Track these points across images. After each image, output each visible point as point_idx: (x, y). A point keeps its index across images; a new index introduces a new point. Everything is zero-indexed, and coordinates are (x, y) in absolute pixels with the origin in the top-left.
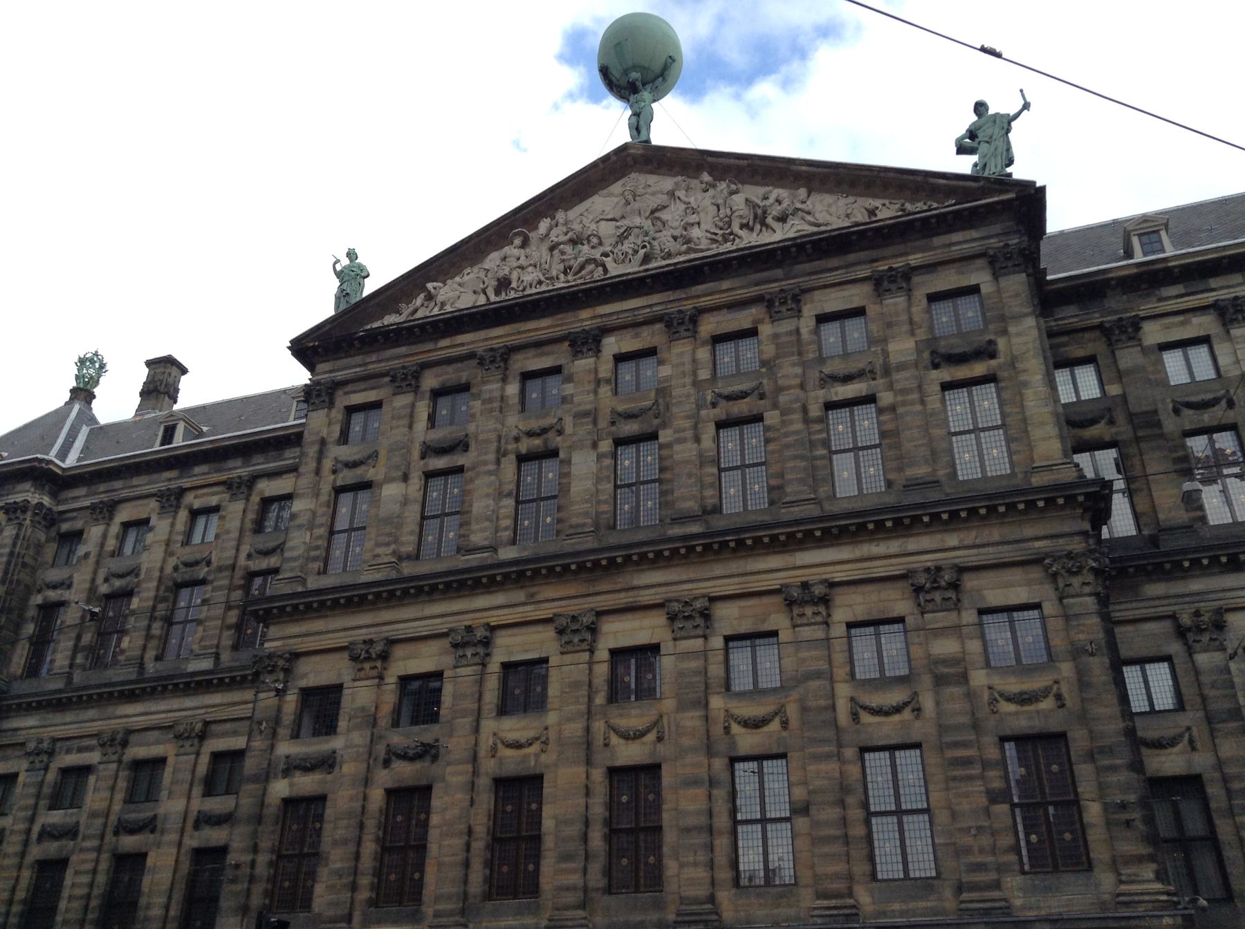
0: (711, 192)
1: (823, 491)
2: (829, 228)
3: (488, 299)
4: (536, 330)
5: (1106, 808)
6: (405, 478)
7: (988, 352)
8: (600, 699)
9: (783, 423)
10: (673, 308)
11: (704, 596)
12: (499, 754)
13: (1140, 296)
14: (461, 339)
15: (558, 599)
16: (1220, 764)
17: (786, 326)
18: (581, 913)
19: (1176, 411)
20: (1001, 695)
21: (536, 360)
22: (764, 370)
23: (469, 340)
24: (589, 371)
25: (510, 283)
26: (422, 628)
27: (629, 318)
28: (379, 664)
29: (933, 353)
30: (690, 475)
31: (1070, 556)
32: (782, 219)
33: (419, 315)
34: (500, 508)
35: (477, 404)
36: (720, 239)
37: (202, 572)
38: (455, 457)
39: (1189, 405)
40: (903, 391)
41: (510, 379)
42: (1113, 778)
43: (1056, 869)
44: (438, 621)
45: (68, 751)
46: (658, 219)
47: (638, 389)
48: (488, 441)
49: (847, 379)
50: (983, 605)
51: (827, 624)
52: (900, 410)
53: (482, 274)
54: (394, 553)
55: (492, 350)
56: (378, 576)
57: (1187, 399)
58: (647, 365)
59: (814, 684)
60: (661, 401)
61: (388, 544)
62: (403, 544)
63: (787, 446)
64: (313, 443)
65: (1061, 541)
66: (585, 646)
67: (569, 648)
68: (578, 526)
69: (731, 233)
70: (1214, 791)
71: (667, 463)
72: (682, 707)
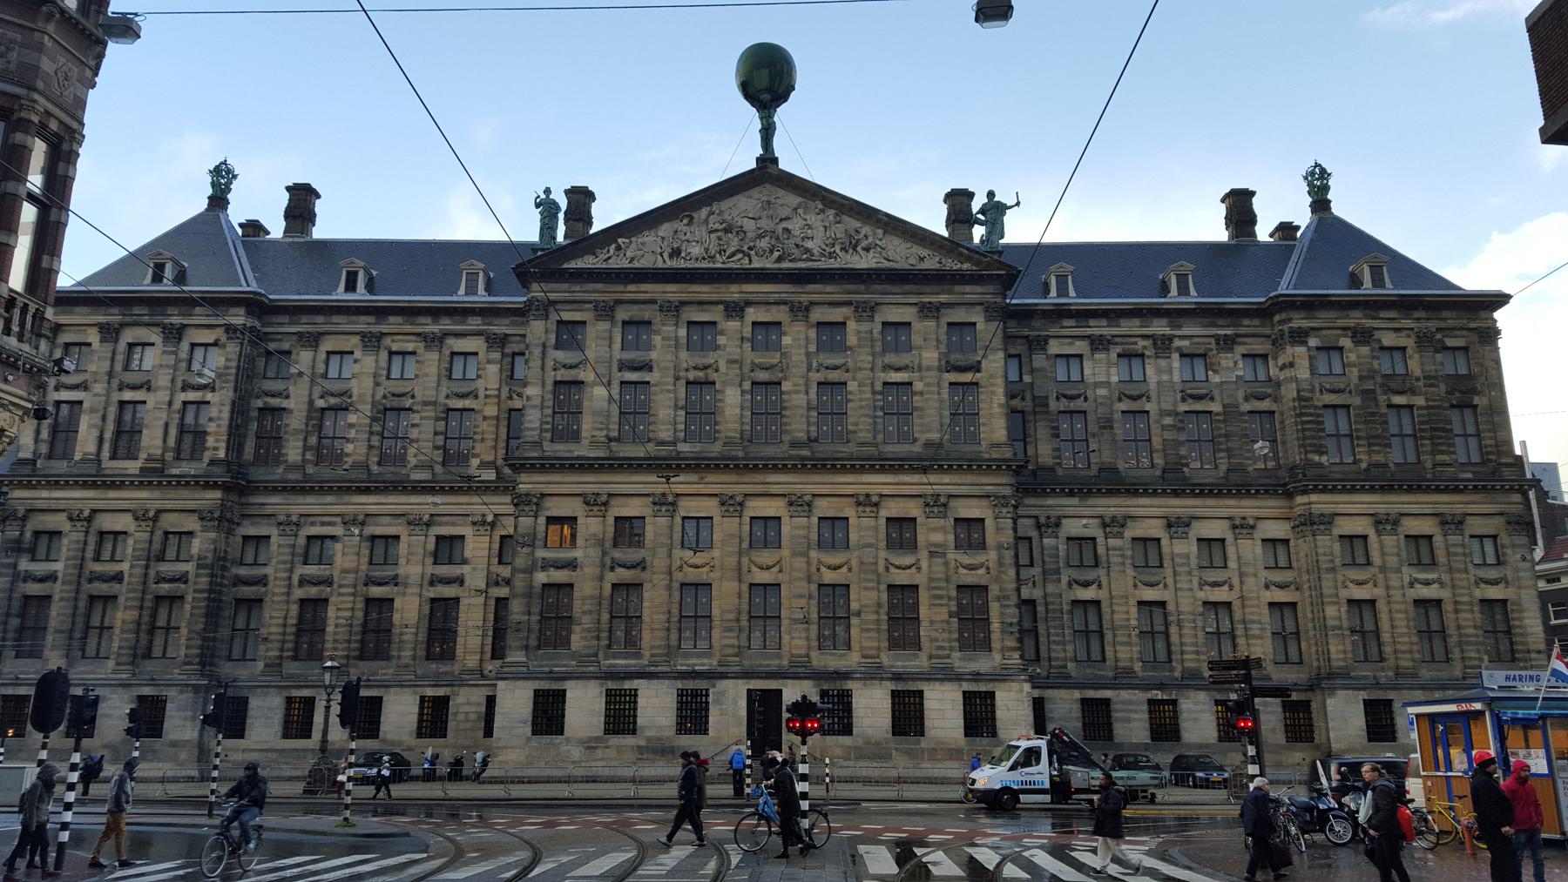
7: (976, 368)
8: (745, 545)
10: (794, 298)
14: (644, 287)
16: (1045, 595)
17: (865, 326)
32: (867, 249)
37: (408, 403)
39: (1065, 396)
40: (929, 385)
45: (313, 524)
48: (667, 368)
49: (898, 369)
70: (1040, 608)
72: (795, 554)
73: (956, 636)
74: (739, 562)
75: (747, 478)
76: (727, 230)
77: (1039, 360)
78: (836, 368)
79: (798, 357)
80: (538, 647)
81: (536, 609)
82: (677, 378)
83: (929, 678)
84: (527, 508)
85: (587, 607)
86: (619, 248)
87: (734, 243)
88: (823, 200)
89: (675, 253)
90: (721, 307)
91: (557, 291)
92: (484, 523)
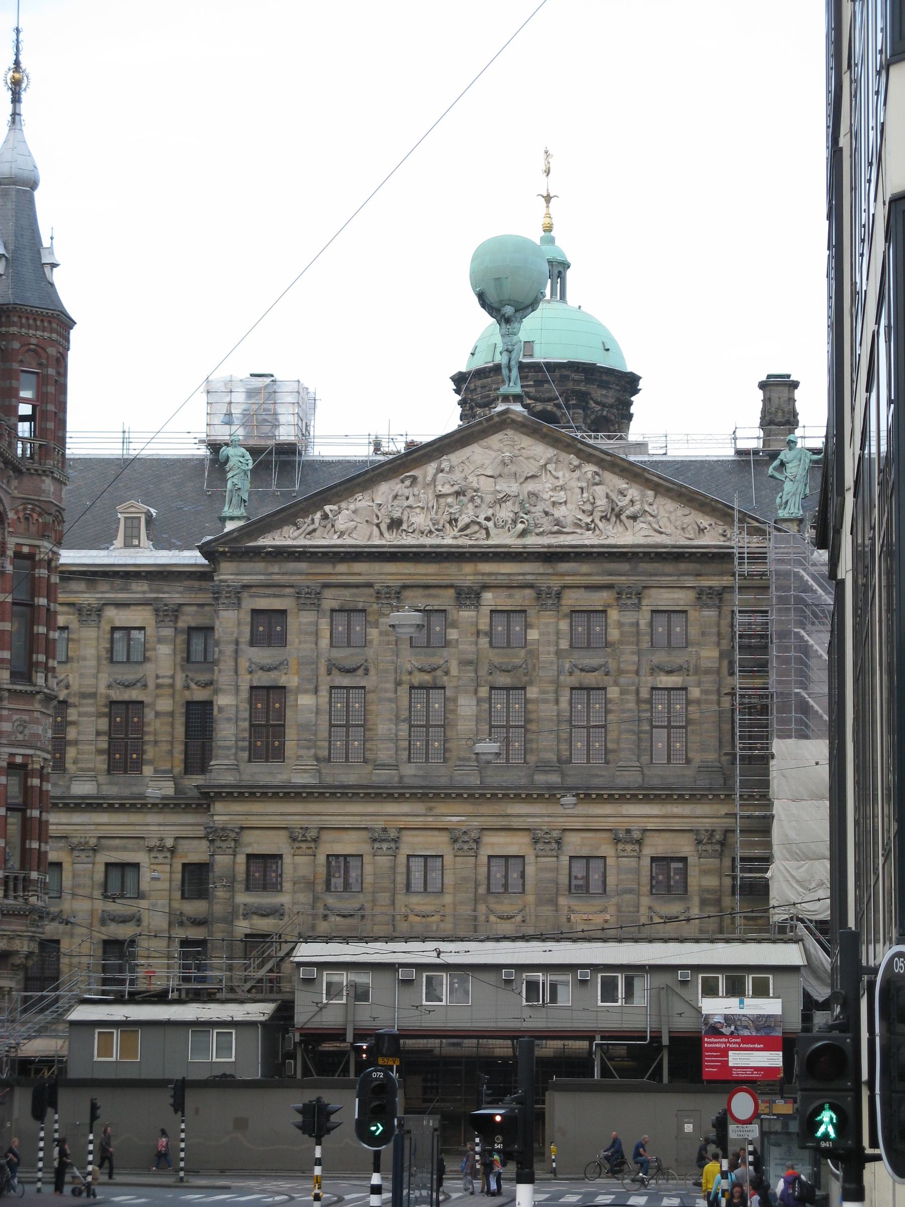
0: (577, 473)
6: (316, 691)
8: (482, 890)
15: (455, 815)
17: (629, 617)
26: (346, 821)
27: (504, 580)
28: (313, 845)
32: (634, 518)
38: (358, 679)
48: (386, 671)
49: (670, 672)
59: (627, 897)
60: (529, 661)
61: (309, 748)
67: (460, 853)
68: (464, 759)
71: (533, 716)
72: (539, 902)
75: (485, 809)
79: (547, 656)
82: (398, 683)
86: (325, 517)
89: (395, 524)
90: (451, 592)
91: (253, 572)
92: (161, 849)
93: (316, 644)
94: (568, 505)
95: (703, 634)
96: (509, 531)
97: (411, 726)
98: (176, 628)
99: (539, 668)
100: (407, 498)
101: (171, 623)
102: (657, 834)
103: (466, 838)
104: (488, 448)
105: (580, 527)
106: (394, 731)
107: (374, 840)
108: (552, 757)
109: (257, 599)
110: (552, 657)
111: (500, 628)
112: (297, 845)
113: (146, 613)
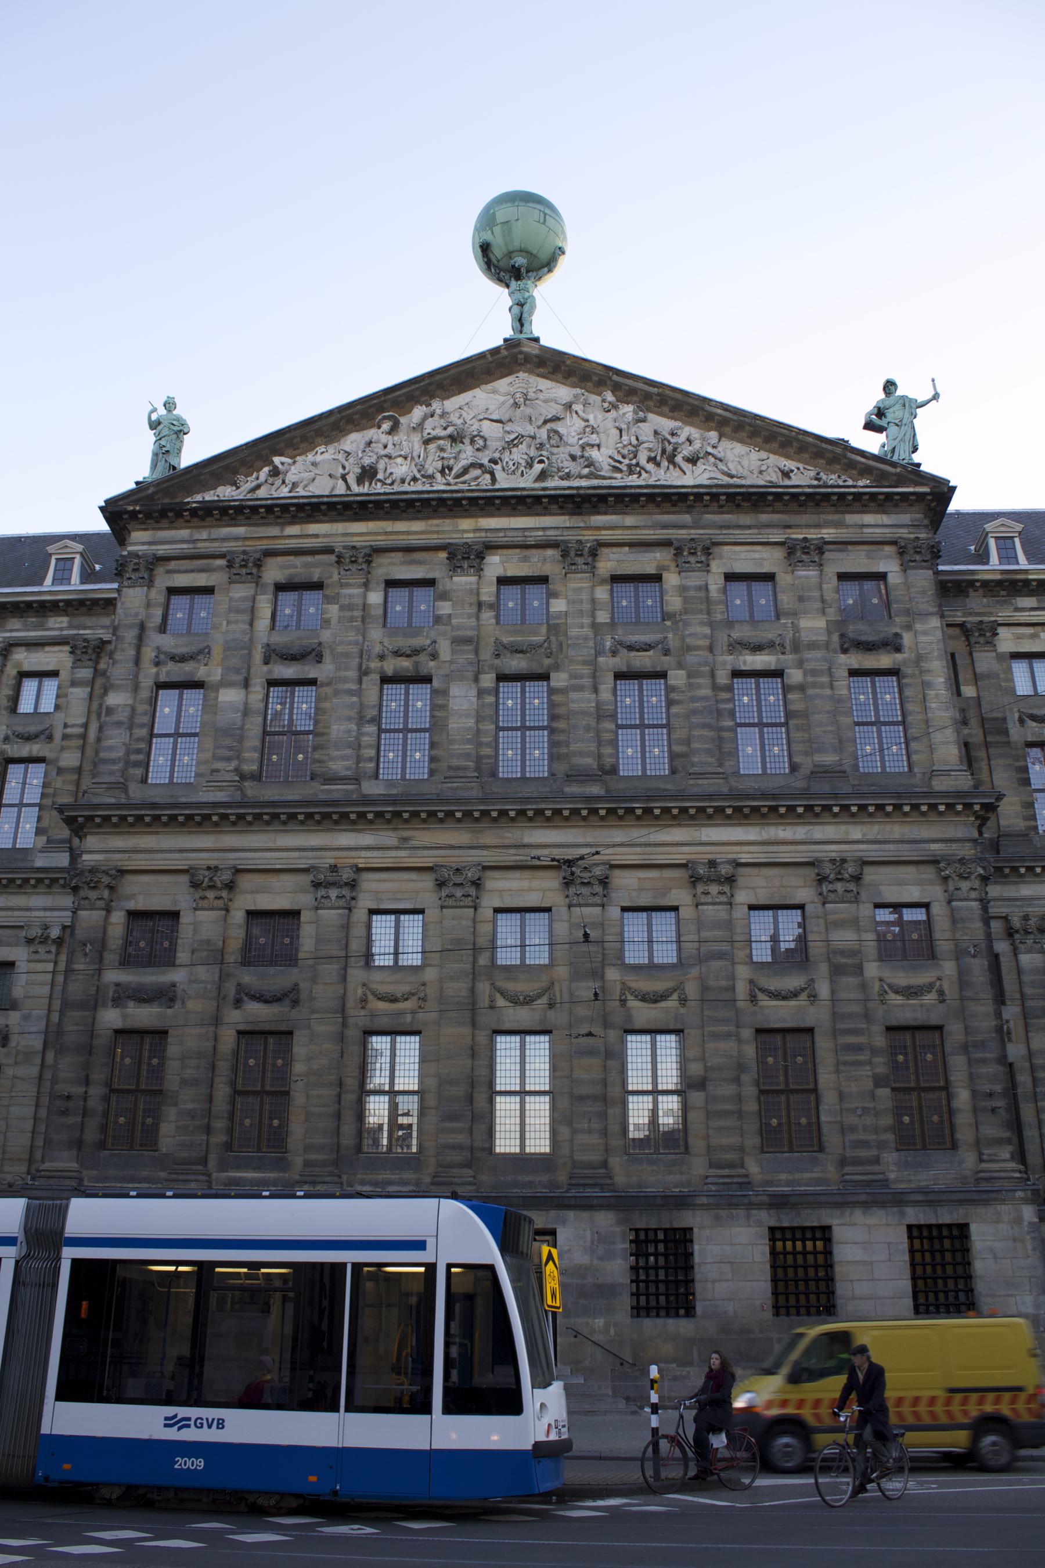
0: (613, 414)
1: (729, 764)
2: (743, 482)
3: (348, 488)
4: (408, 533)
5: (974, 1094)
6: (246, 684)
7: (894, 645)
9: (691, 686)
10: (571, 537)
11: (604, 864)
12: (369, 1006)
13: (998, 602)
14: (313, 528)
16: (1030, 1054)
17: (694, 580)
18: (468, 1172)
19: (1021, 721)
20: (890, 986)
21: (404, 568)
22: (668, 623)
23: (322, 530)
24: (471, 591)
25: (376, 473)
26: (276, 860)
28: (224, 894)
29: (842, 636)
30: (588, 729)
31: (962, 861)
32: (693, 460)
33: (262, 493)
34: (363, 734)
35: (333, 609)
36: (625, 468)
38: (306, 668)
39: (1034, 718)
40: (814, 672)
41: (372, 585)
42: (983, 1070)
43: (924, 1148)
44: (296, 854)
46: (556, 432)
47: (523, 621)
48: (347, 655)
49: (757, 648)
50: (879, 900)
51: (731, 904)
52: (810, 692)
53: (341, 457)
54: (237, 770)
55: (354, 547)
56: (220, 796)
57: (1031, 712)
58: (535, 596)
59: (716, 964)
60: (553, 638)
61: (229, 759)
62: (246, 760)
63: (694, 712)
64: (130, 626)
65: (954, 846)
66: (468, 901)
67: (450, 902)
68: (457, 768)
69: (637, 465)
71: (562, 711)
73: (887, 1121)
74: (472, 990)
75: (489, 837)
76: (455, 439)
77: (985, 661)
78: (647, 647)
80: (102, 1145)
81: (98, 1075)
83: (842, 1203)
84: (93, 895)
85: (189, 1073)
87: (468, 454)
88: (616, 388)
90: (443, 555)
91: (173, 539)
92: (44, 940)
93: (251, 624)
94: (602, 449)
95: (801, 599)
96: (522, 475)
97: (380, 731)
98: (96, 670)
99: (568, 646)
100: (385, 447)
101: (90, 663)
102: (755, 871)
103: (459, 880)
104: (494, 392)
105: (620, 471)
106: (354, 734)
107: (317, 885)
108: (589, 761)
109: (175, 575)
110: (587, 631)
111: (511, 604)
112: (201, 893)
113: (62, 655)
